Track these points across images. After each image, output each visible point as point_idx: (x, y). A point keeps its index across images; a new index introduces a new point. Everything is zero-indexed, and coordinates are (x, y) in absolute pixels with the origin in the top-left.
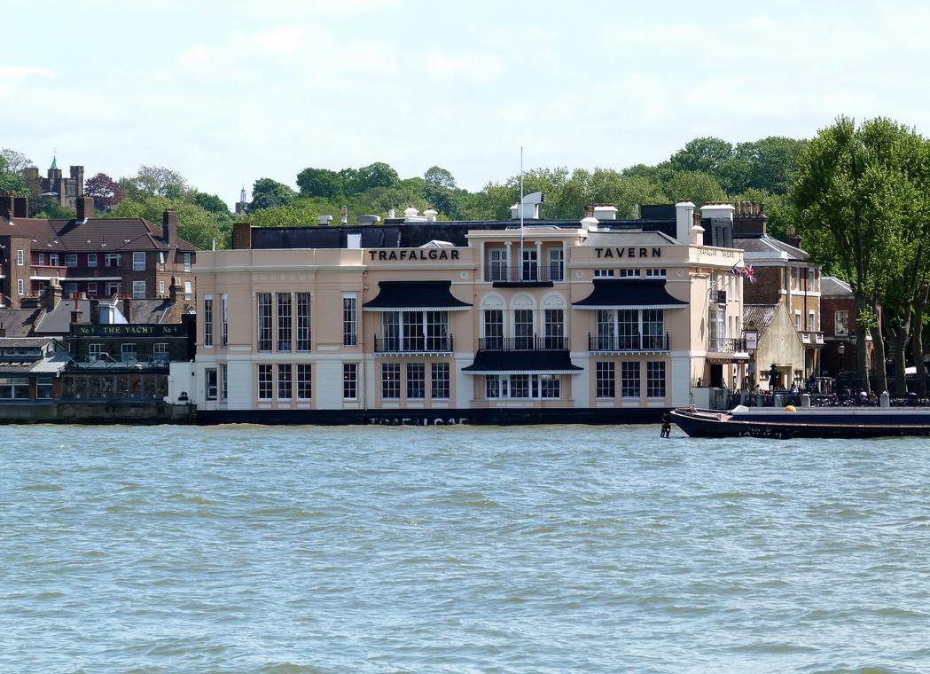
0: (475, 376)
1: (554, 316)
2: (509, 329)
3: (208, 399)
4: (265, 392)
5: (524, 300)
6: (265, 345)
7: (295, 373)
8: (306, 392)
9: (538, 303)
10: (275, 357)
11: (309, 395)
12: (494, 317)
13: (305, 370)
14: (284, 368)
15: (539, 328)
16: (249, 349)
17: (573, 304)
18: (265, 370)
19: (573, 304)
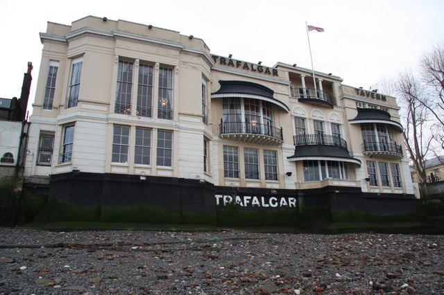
0: (297, 163)
1: (336, 126)
2: (310, 129)
3: (37, 165)
4: (119, 152)
5: (318, 114)
6: (122, 108)
7: (154, 137)
8: (165, 158)
9: (330, 116)
10: (132, 119)
11: (168, 163)
12: (300, 120)
13: (166, 136)
14: (144, 132)
15: (328, 130)
16: (105, 108)
17: (349, 121)
18: (120, 130)
19: (349, 121)
